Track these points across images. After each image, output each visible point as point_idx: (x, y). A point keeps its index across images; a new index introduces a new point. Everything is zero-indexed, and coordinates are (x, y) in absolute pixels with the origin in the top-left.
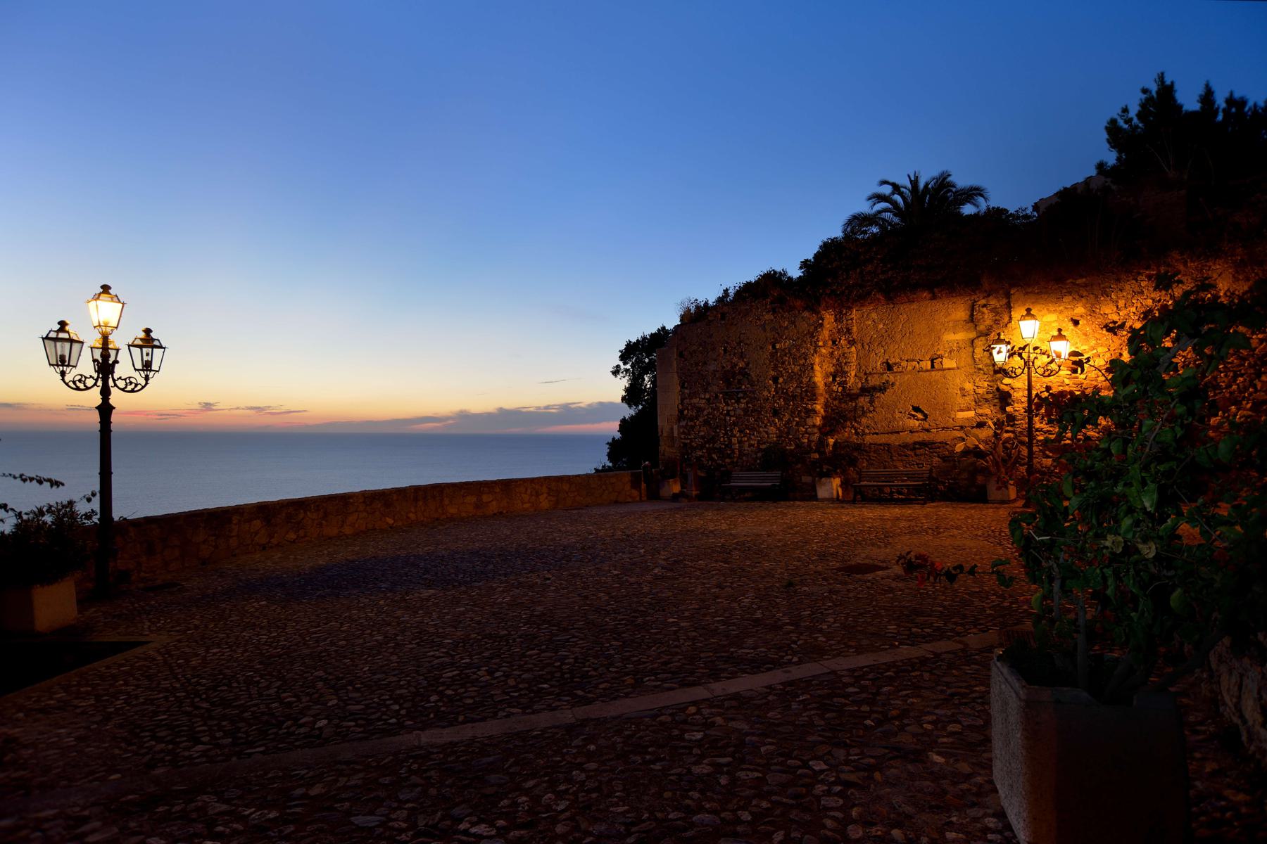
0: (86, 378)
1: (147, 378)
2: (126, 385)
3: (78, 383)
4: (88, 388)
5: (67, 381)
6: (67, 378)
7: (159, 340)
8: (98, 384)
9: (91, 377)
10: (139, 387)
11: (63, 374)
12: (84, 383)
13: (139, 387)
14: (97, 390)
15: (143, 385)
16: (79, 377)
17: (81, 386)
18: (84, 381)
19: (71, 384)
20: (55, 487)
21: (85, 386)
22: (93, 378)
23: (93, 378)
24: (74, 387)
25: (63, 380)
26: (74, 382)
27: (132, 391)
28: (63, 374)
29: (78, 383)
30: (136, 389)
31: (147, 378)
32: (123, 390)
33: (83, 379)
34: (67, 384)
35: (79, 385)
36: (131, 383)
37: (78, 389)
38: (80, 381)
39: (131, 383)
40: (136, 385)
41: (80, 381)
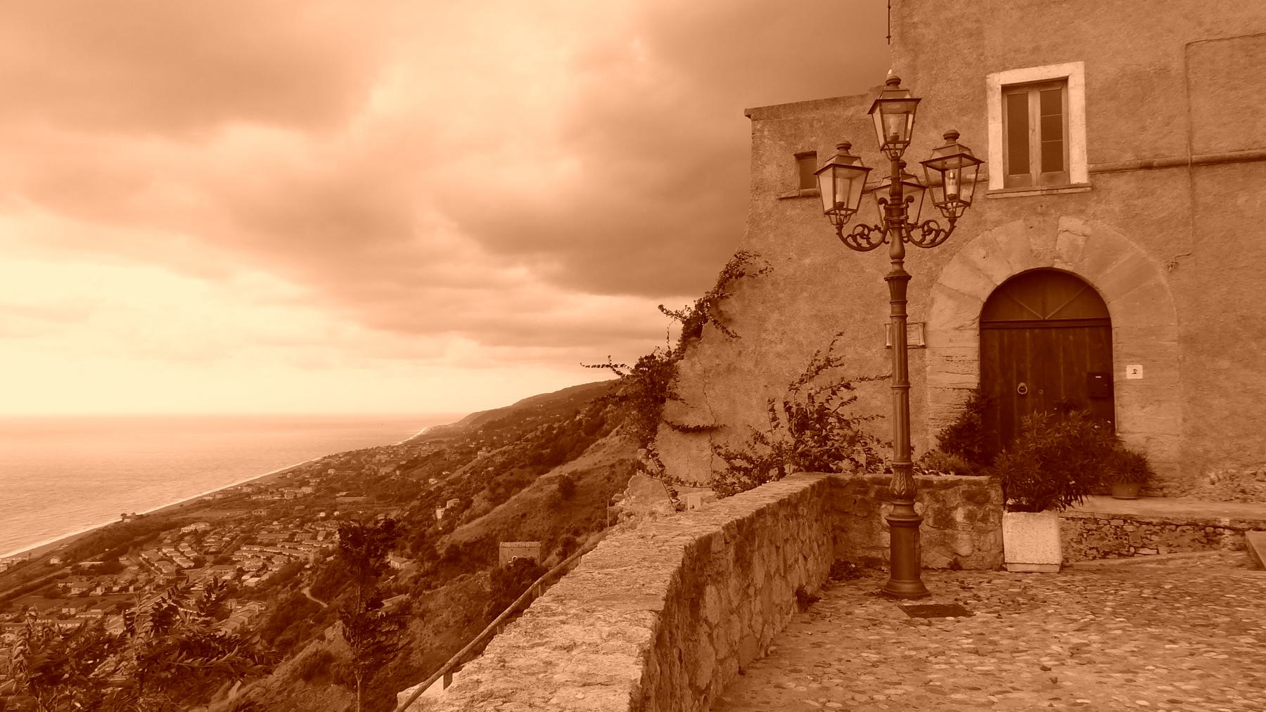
0: (870, 230)
1: (953, 220)
2: (924, 236)
4: (873, 247)
5: (845, 236)
6: (846, 232)
10: (942, 235)
11: (840, 226)
12: (868, 239)
15: (947, 230)
16: (860, 229)
17: (864, 243)
18: (868, 235)
19: (850, 240)
21: (869, 243)
22: (879, 229)
23: (879, 229)
24: (855, 245)
25: (840, 234)
26: (855, 240)
27: (933, 244)
28: (840, 226)
30: (938, 239)
31: (953, 220)
32: (919, 244)
33: (866, 232)
34: (845, 240)
35: (860, 242)
36: (930, 231)
37: (860, 248)
38: (862, 235)
39: (930, 231)
40: (938, 232)
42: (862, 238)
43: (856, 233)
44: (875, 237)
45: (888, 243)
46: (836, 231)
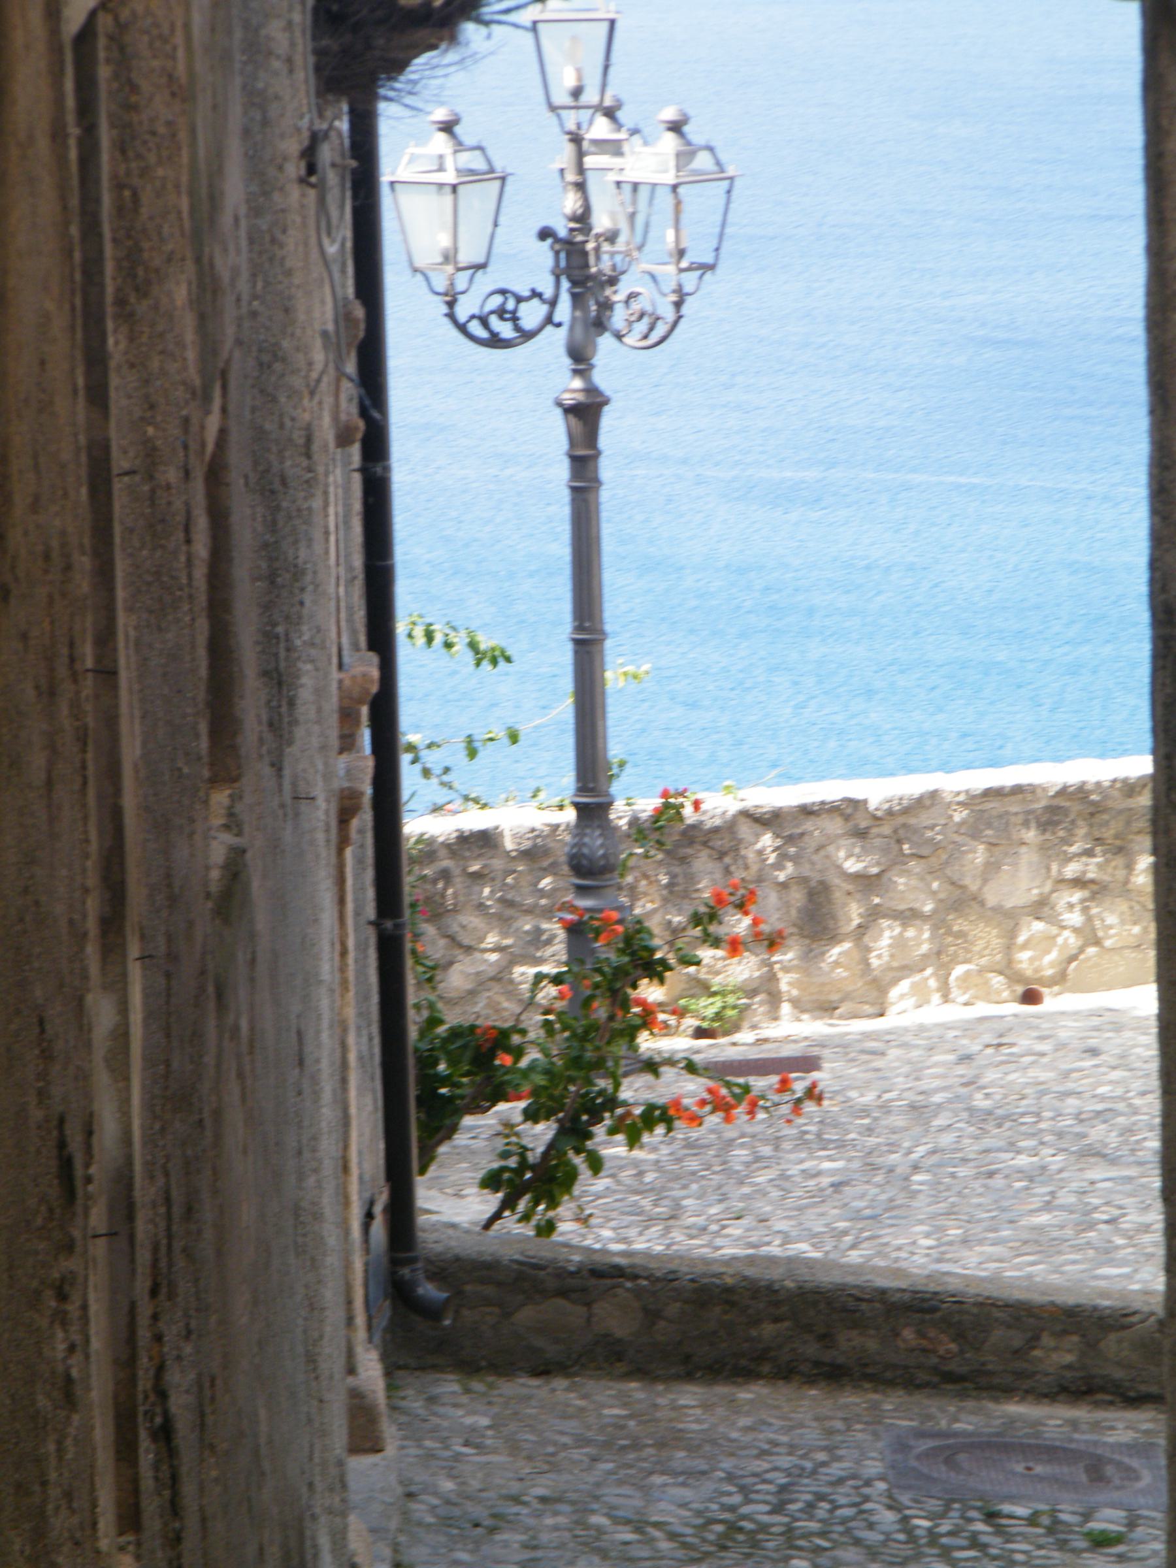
0: (519, 299)
3: (494, 321)
4: (527, 336)
5: (462, 316)
6: (463, 311)
7: (711, 149)
8: (557, 318)
9: (535, 294)
10: (660, 330)
12: (515, 319)
13: (660, 330)
14: (554, 341)
16: (496, 301)
17: (505, 330)
18: (514, 312)
19: (476, 328)
20: (486, 665)
21: (517, 328)
24: (482, 333)
25: (451, 316)
26: (484, 322)
29: (494, 321)
30: (655, 336)
33: (511, 305)
34: (462, 328)
37: (495, 341)
38: (501, 313)
41: (501, 313)
42: (502, 318)
43: (487, 309)
44: (531, 314)
45: (559, 325)
46: (444, 309)
